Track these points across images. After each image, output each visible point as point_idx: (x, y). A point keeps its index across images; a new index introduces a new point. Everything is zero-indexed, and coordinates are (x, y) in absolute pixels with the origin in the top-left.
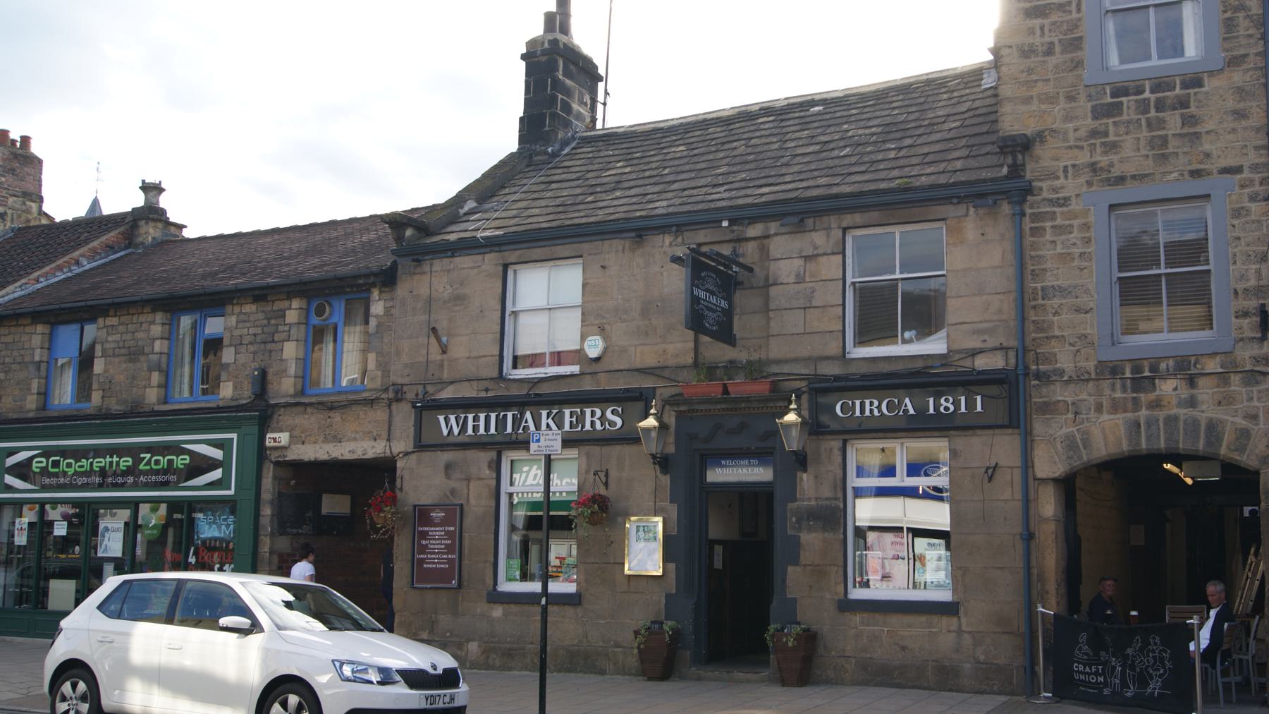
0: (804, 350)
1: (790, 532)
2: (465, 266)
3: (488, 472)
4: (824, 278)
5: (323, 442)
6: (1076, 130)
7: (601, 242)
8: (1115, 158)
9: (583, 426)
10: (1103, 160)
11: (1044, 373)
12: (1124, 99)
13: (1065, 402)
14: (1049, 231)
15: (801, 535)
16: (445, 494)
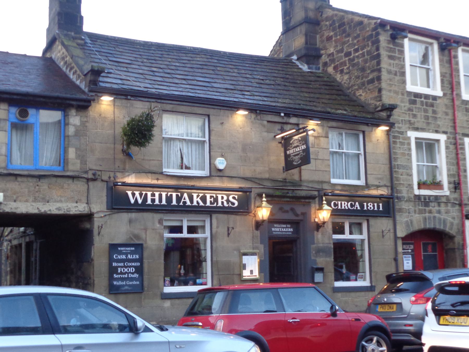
0: (316, 178)
1: (313, 258)
2: (138, 107)
3: (158, 225)
4: (322, 147)
5: (33, 201)
6: (404, 107)
7: (219, 110)
8: (416, 120)
9: (217, 204)
10: (413, 120)
11: (399, 197)
12: (417, 99)
13: (406, 209)
14: (398, 143)
15: (317, 259)
16: (130, 237)
